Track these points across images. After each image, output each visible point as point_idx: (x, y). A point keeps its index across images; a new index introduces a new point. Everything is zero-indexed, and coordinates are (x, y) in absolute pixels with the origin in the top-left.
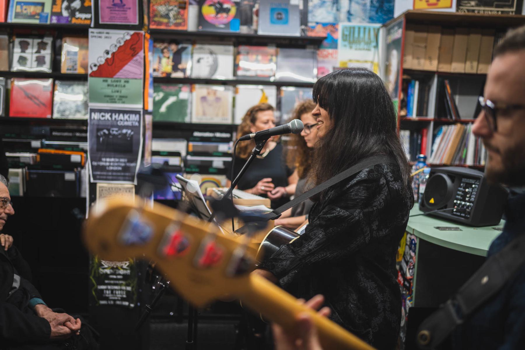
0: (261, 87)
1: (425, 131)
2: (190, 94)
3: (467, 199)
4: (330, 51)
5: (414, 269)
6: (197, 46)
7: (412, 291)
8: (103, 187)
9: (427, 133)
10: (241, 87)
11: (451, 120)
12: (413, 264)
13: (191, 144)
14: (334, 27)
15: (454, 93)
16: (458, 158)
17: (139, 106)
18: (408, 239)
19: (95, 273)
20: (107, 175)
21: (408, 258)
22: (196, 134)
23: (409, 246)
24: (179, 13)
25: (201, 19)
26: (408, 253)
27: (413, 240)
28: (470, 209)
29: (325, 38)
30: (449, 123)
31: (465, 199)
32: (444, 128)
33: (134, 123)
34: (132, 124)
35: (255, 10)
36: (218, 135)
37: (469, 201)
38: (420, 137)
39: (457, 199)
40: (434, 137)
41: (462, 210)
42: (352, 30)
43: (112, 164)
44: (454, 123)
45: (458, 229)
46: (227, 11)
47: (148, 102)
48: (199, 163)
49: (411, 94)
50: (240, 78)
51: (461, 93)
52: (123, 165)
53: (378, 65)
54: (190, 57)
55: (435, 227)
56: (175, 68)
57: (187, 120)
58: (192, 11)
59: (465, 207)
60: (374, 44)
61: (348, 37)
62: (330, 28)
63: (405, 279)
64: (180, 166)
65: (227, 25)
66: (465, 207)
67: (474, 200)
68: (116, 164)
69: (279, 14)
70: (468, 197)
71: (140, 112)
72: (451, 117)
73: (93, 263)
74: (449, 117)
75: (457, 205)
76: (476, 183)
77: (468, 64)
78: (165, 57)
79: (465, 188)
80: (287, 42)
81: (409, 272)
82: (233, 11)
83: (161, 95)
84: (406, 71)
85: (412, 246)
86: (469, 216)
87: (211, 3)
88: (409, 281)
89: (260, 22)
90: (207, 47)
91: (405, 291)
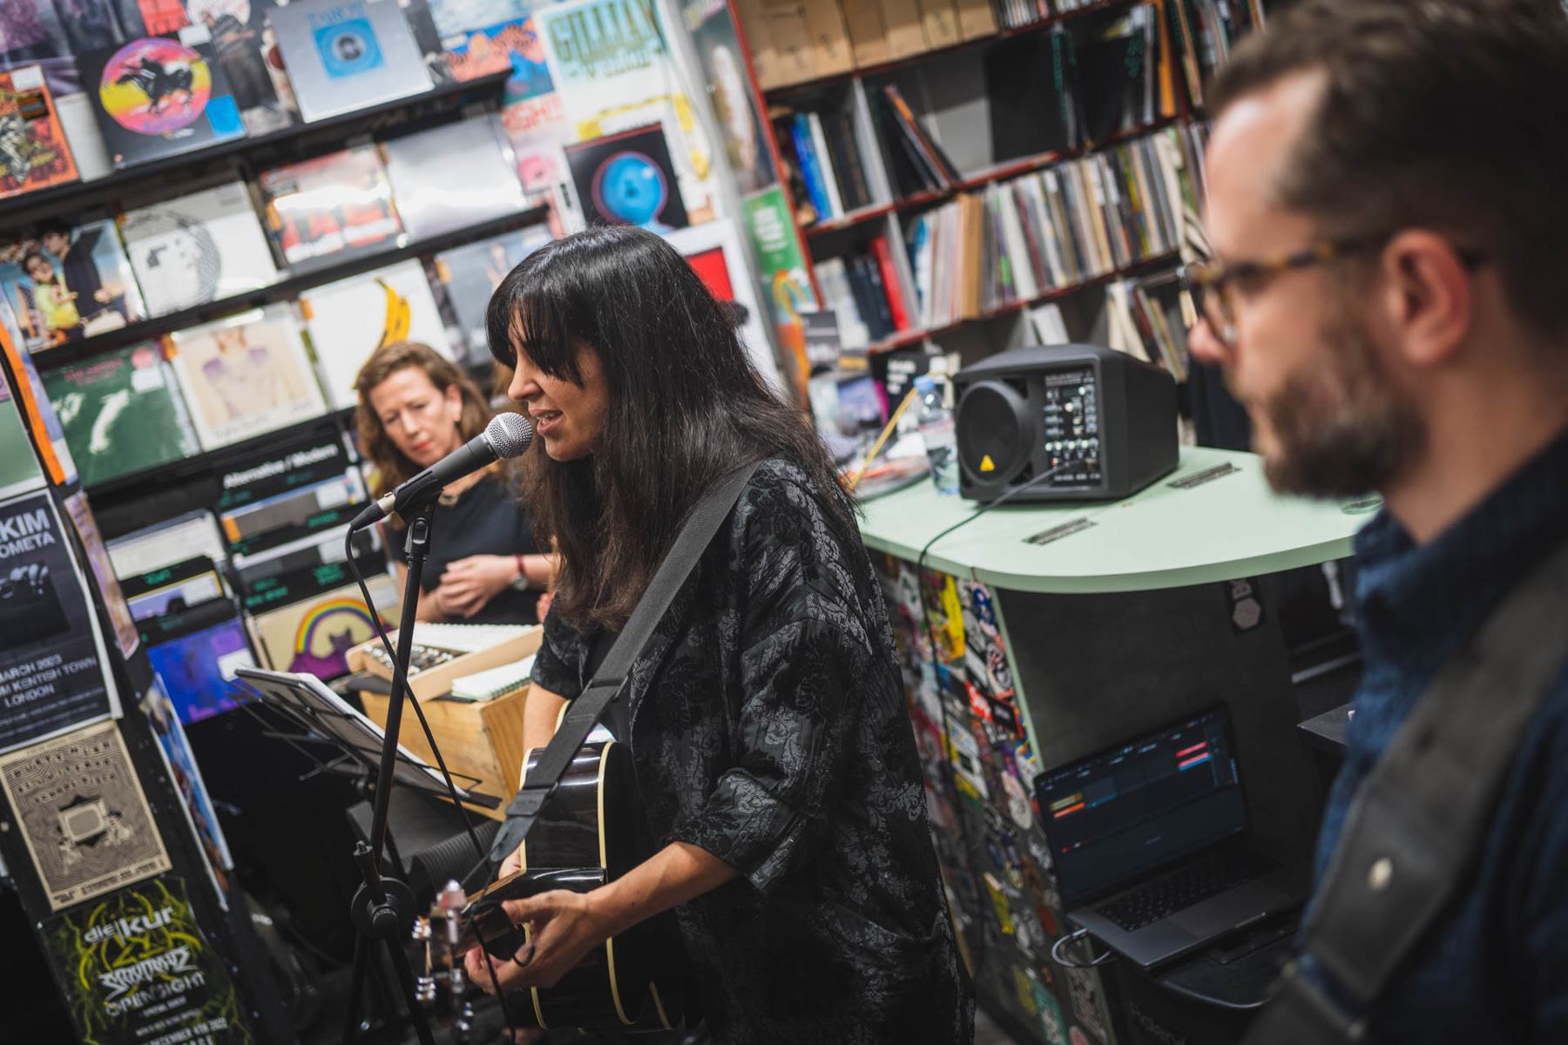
0: (372, 275)
1: (880, 245)
2: (165, 367)
3: (1077, 431)
4: (537, 102)
5: (1007, 671)
6: (131, 217)
7: (1024, 731)
8: (15, 764)
9: (888, 249)
10: (315, 297)
11: (939, 194)
12: (1001, 656)
13: (228, 517)
14: (520, 29)
15: (919, 110)
16: (993, 290)
17: (35, 482)
18: (965, 594)
19: (93, 1020)
20: (15, 726)
21: (982, 643)
22: (231, 481)
23: (972, 610)
24: (31, 135)
25: (108, 129)
26: (974, 629)
27: (978, 591)
28: (1094, 454)
29: (510, 72)
30: (936, 203)
31: (1072, 431)
32: (930, 220)
33: (37, 538)
34: (34, 542)
35: (265, 51)
36: (300, 459)
37: (1085, 436)
38: (872, 266)
39: (1052, 439)
40: (911, 251)
41: (1076, 462)
42: (576, 21)
43: (16, 686)
44: (949, 197)
45: (1084, 524)
46: (183, 80)
47: (54, 458)
48: (279, 568)
49: (808, 153)
50: (300, 271)
51: (939, 106)
52: (53, 674)
53: (687, 101)
54: (120, 255)
55: (1024, 541)
56: (88, 306)
57: (189, 448)
58: (72, 113)
59: (1080, 455)
60: (654, 43)
61: (573, 47)
62: (510, 36)
63: (992, 701)
64: (223, 597)
65: (200, 123)
66: (1080, 455)
67: (1098, 428)
68: (30, 681)
69: (345, 41)
70: (1078, 425)
71: (44, 497)
72: (937, 185)
73: (77, 997)
74: (931, 187)
75: (1057, 454)
76: (1085, 380)
77: (930, 22)
78: (40, 282)
79: (1062, 401)
80: (400, 117)
81: (997, 679)
82: (202, 76)
83: (75, 401)
84: (772, 97)
85: (980, 610)
86: (1097, 476)
87: (125, 72)
88: (1006, 703)
89: (297, 84)
90: (161, 209)
91: (1004, 732)
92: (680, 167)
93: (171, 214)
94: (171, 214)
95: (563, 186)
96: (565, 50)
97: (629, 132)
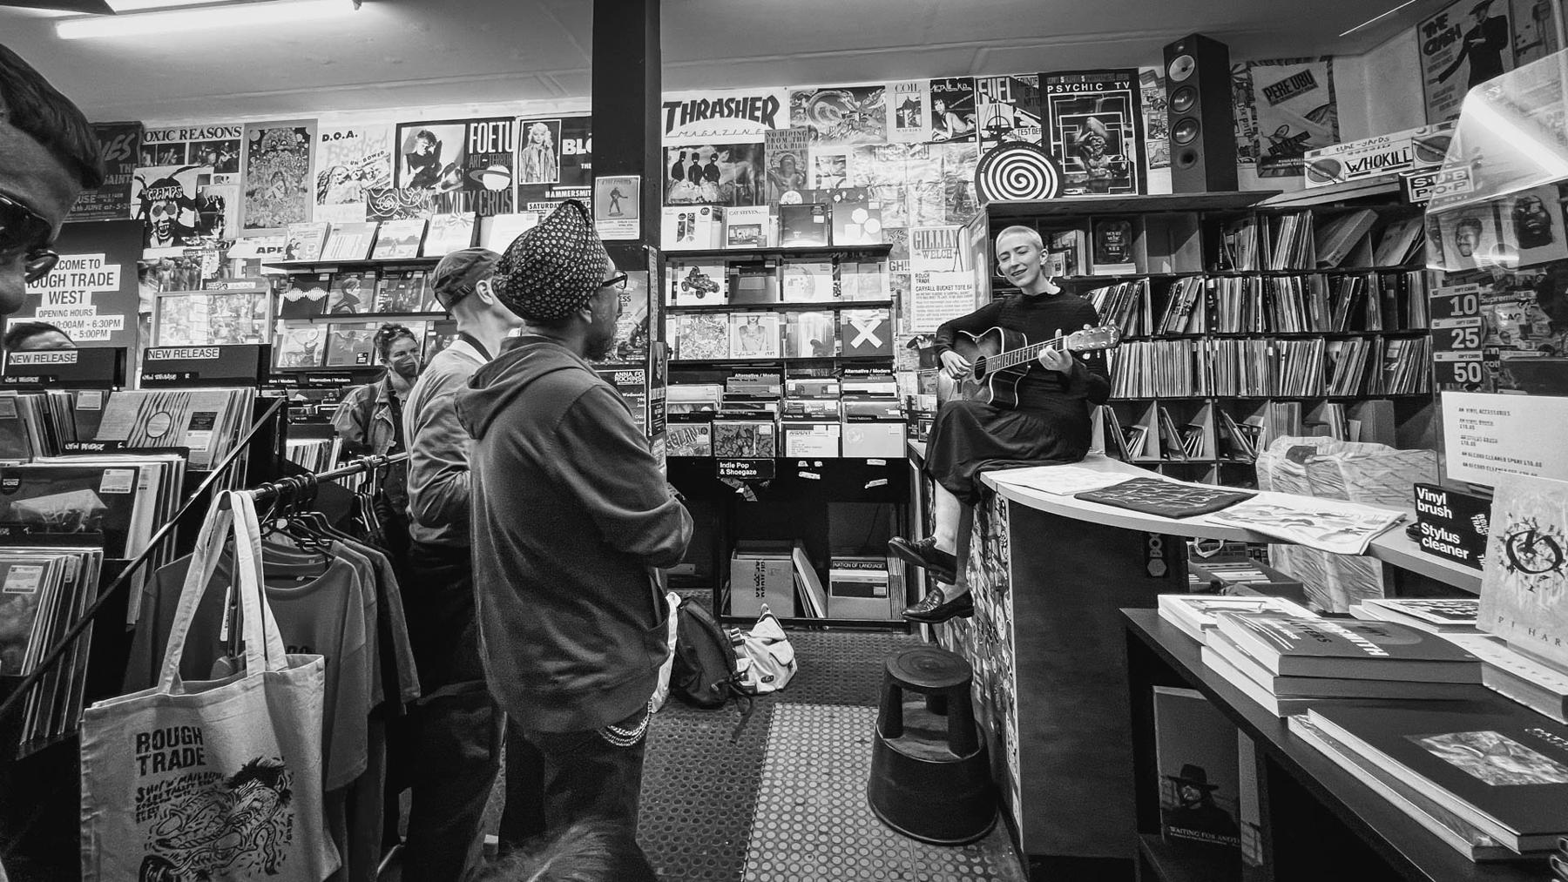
60: (954, 250)
96: (917, 245)
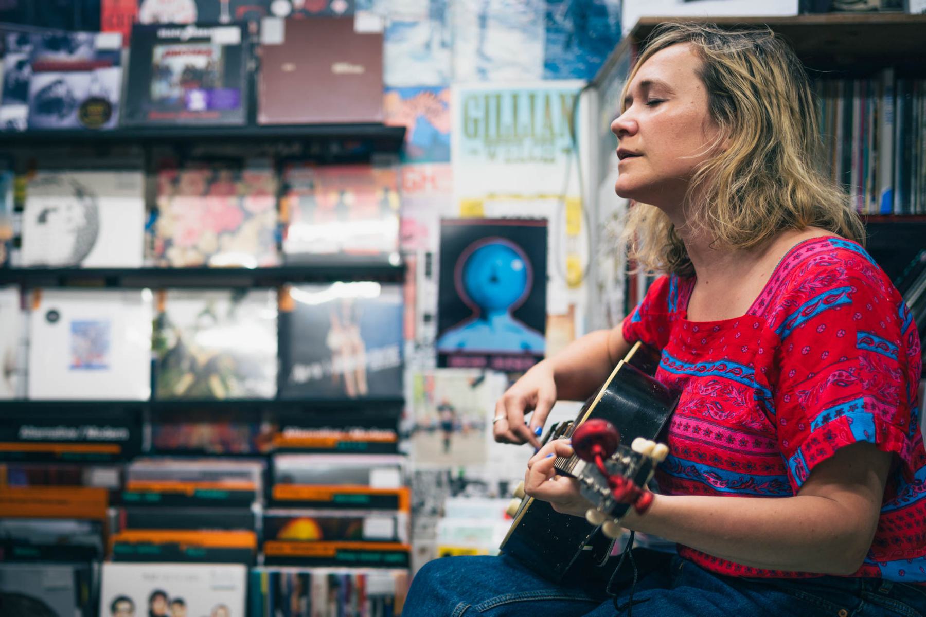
4: (428, 169)
14: (436, 97)
90: (68, 177)
92: (552, 269)
93: (74, 183)
94: (74, 183)
95: (428, 255)
97: (511, 220)
